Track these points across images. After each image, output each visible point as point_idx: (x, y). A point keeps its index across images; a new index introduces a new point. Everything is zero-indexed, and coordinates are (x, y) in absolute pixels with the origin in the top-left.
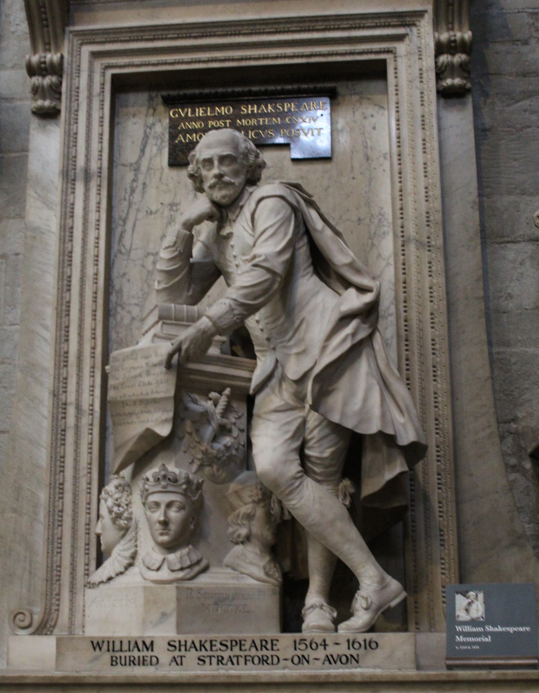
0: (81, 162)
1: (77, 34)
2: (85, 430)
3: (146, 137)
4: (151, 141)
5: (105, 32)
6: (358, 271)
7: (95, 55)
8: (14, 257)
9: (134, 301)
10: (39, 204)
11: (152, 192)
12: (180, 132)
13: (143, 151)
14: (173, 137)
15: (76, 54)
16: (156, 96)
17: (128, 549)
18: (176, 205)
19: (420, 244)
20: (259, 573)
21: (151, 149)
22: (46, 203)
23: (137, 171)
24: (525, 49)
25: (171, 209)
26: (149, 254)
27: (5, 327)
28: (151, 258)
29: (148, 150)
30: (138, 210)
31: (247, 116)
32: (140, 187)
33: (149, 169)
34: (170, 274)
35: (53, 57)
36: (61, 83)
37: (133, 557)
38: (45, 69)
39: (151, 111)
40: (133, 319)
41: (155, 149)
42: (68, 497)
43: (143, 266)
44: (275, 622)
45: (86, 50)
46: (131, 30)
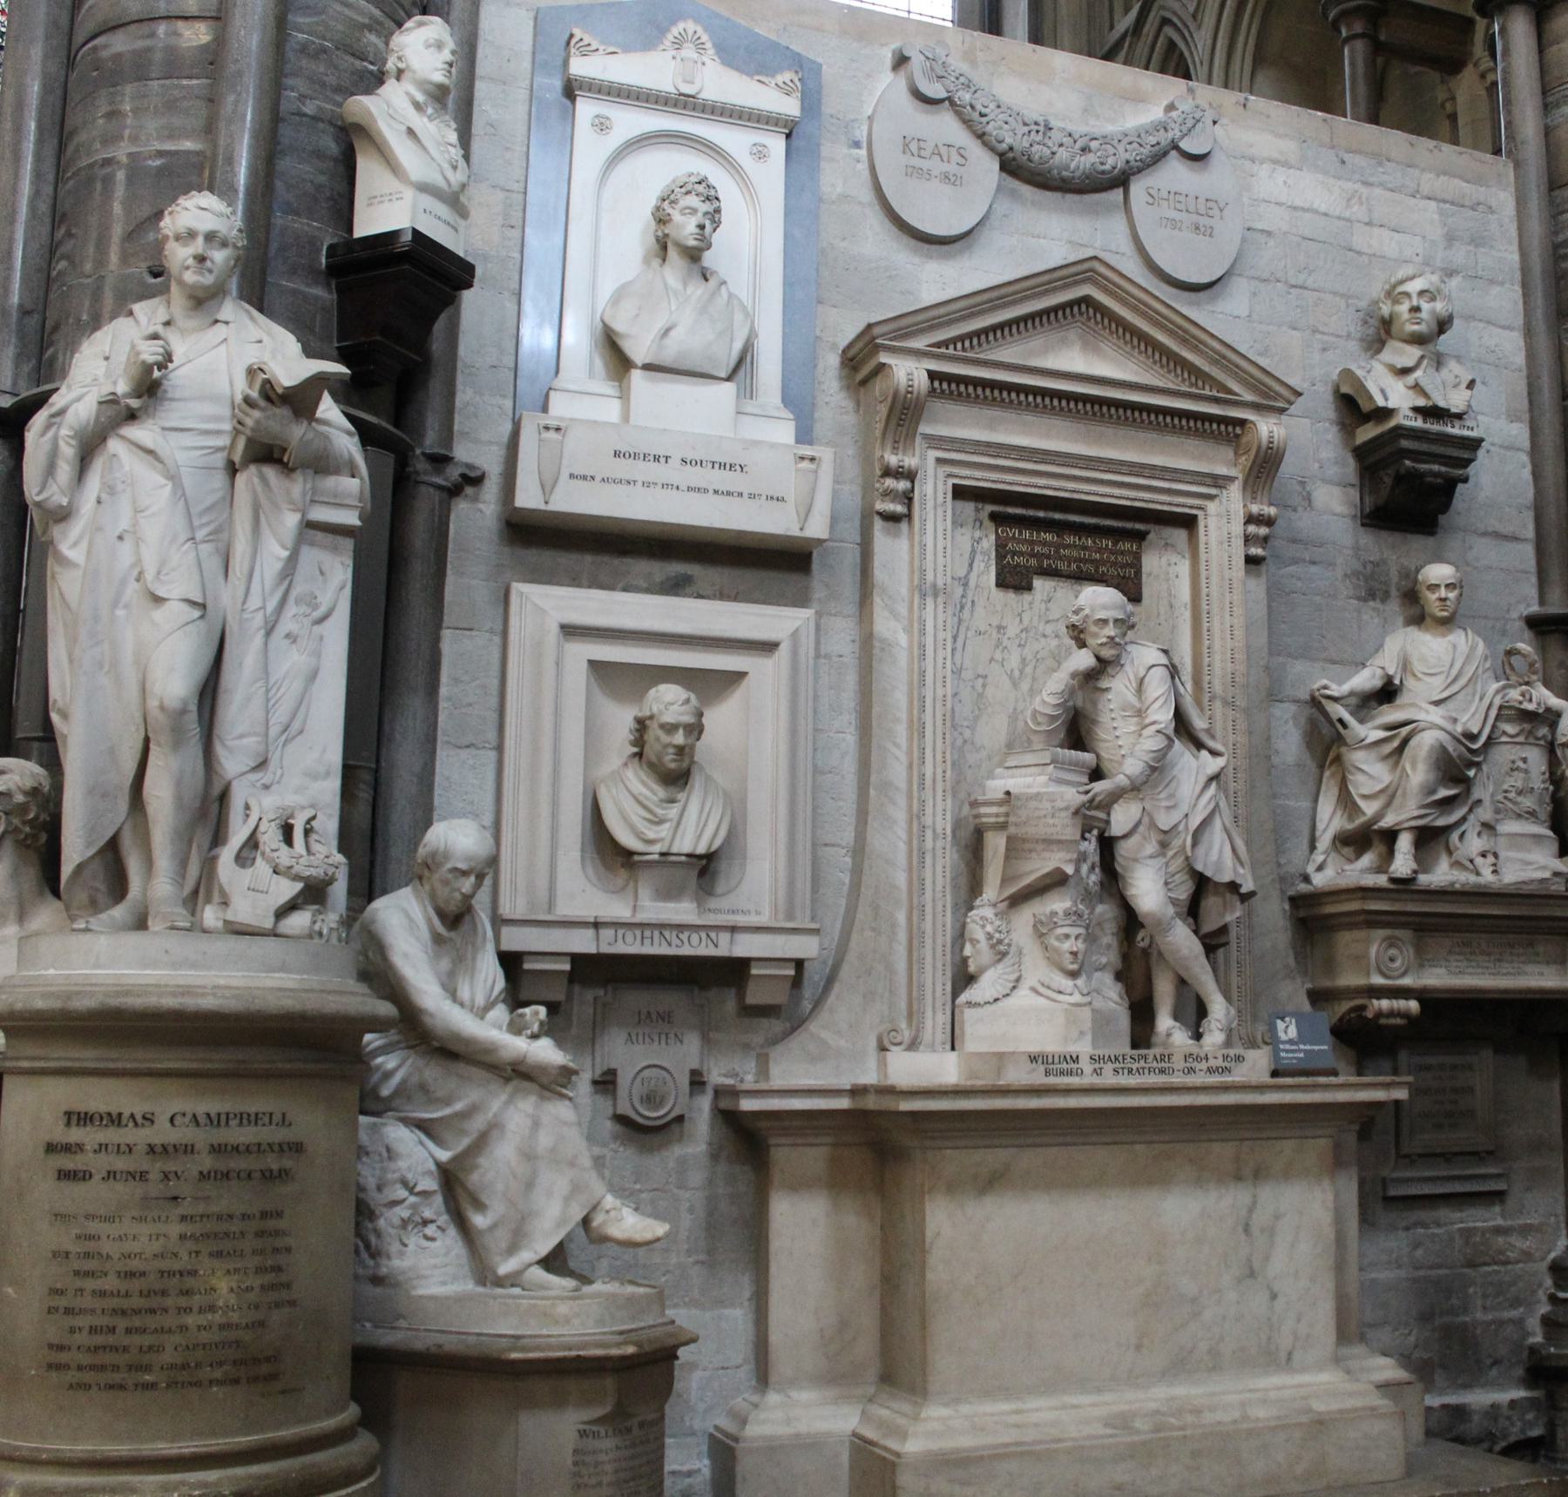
0: (930, 577)
1: (926, 437)
2: (939, 853)
3: (973, 552)
4: (979, 557)
5: (953, 440)
6: (1213, 737)
7: (939, 461)
8: (837, 659)
9: (965, 724)
10: (886, 614)
11: (979, 610)
12: (1008, 552)
13: (971, 565)
14: (1000, 556)
15: (923, 458)
16: (983, 509)
17: (1012, 972)
18: (1004, 628)
19: (1225, 703)
20: (1115, 996)
21: (979, 565)
22: (895, 615)
23: (966, 585)
24: (1294, 516)
25: (999, 632)
26: (979, 676)
27: (831, 734)
28: (980, 681)
29: (975, 565)
30: (968, 629)
31: (1068, 546)
32: (969, 604)
33: (977, 586)
34: (1053, 718)
35: (910, 461)
36: (913, 487)
37: (1018, 980)
38: (902, 473)
39: (978, 524)
40: (965, 742)
41: (983, 565)
42: (929, 918)
43: (973, 687)
44: (1127, 1040)
45: (933, 454)
46: (978, 443)
